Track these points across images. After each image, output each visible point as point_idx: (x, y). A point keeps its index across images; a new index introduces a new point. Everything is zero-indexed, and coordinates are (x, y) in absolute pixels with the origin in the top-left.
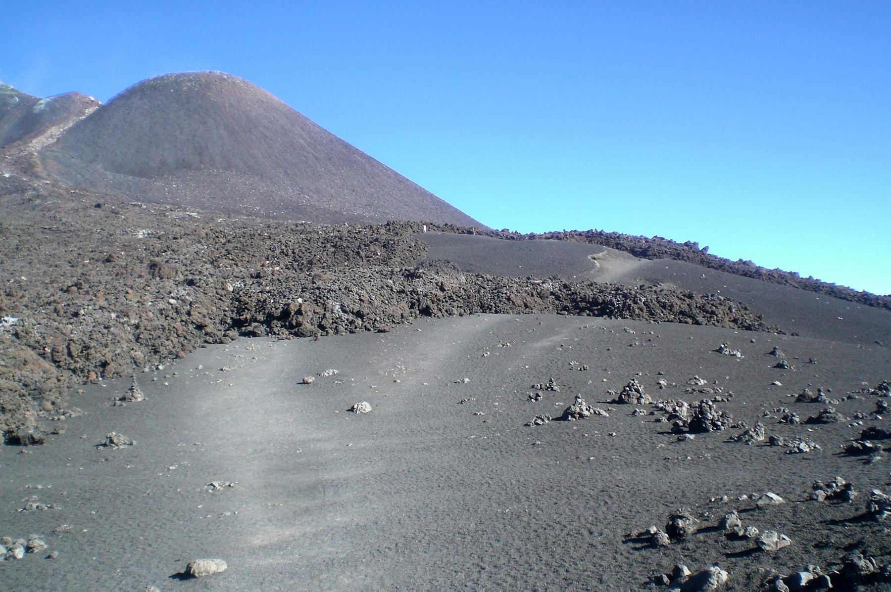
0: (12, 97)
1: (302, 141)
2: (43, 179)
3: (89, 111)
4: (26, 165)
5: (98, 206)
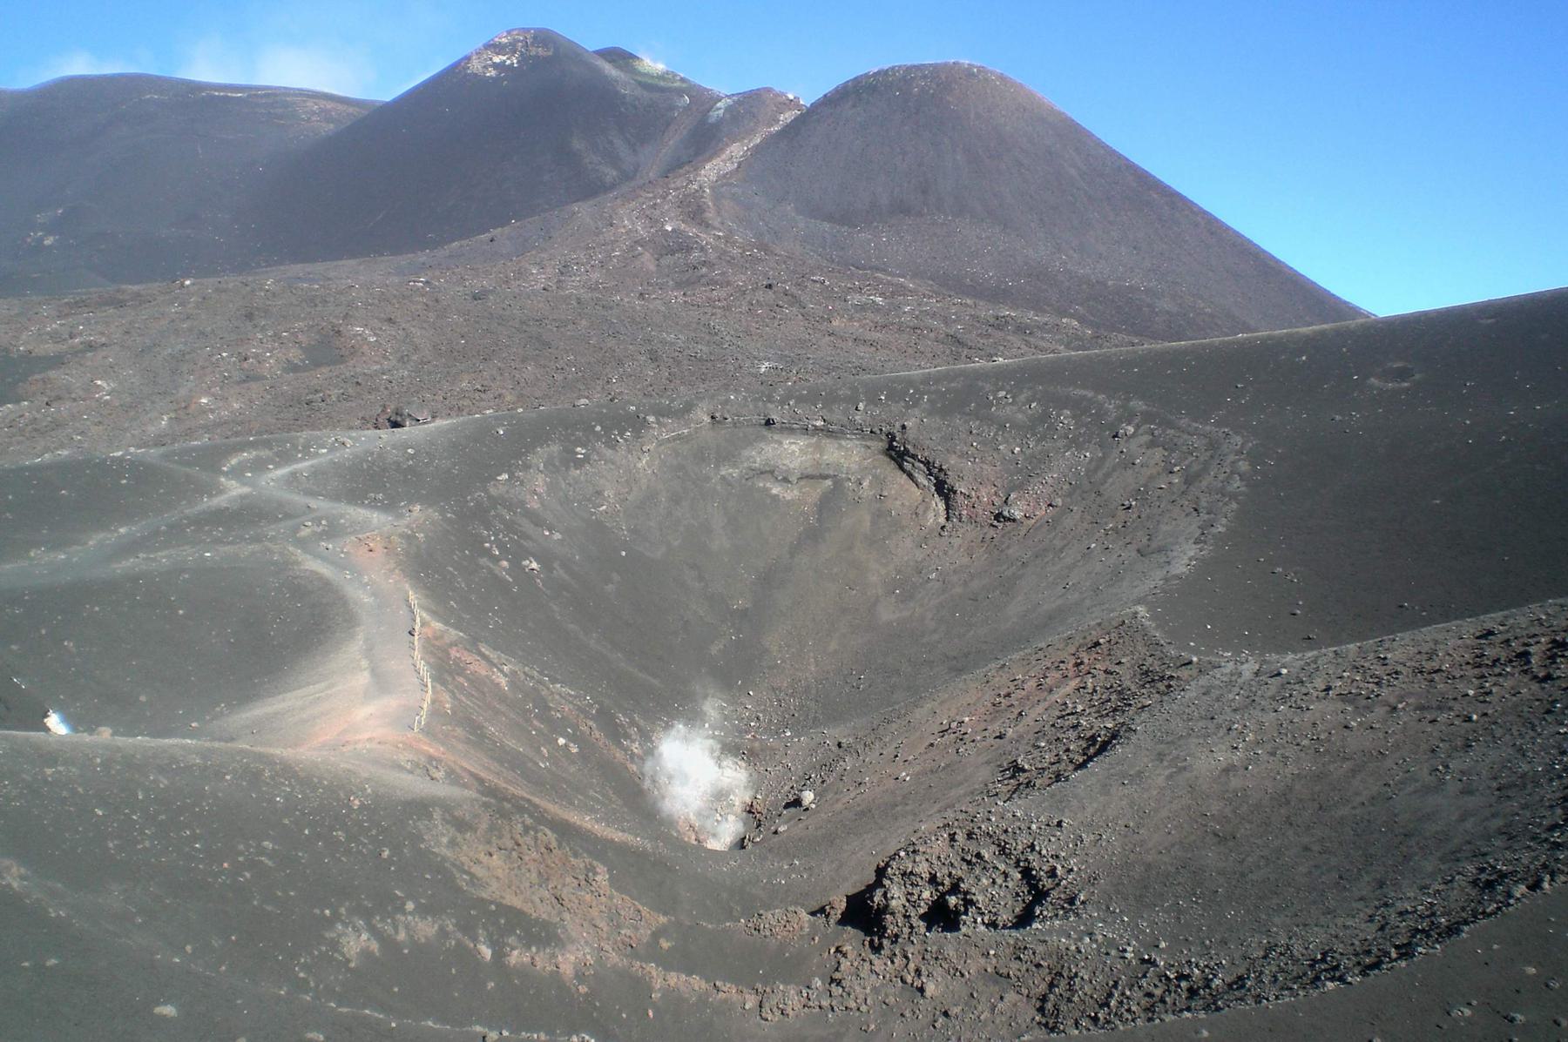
0: (680, 92)
1: (1073, 171)
3: (787, 117)
5: (770, 286)
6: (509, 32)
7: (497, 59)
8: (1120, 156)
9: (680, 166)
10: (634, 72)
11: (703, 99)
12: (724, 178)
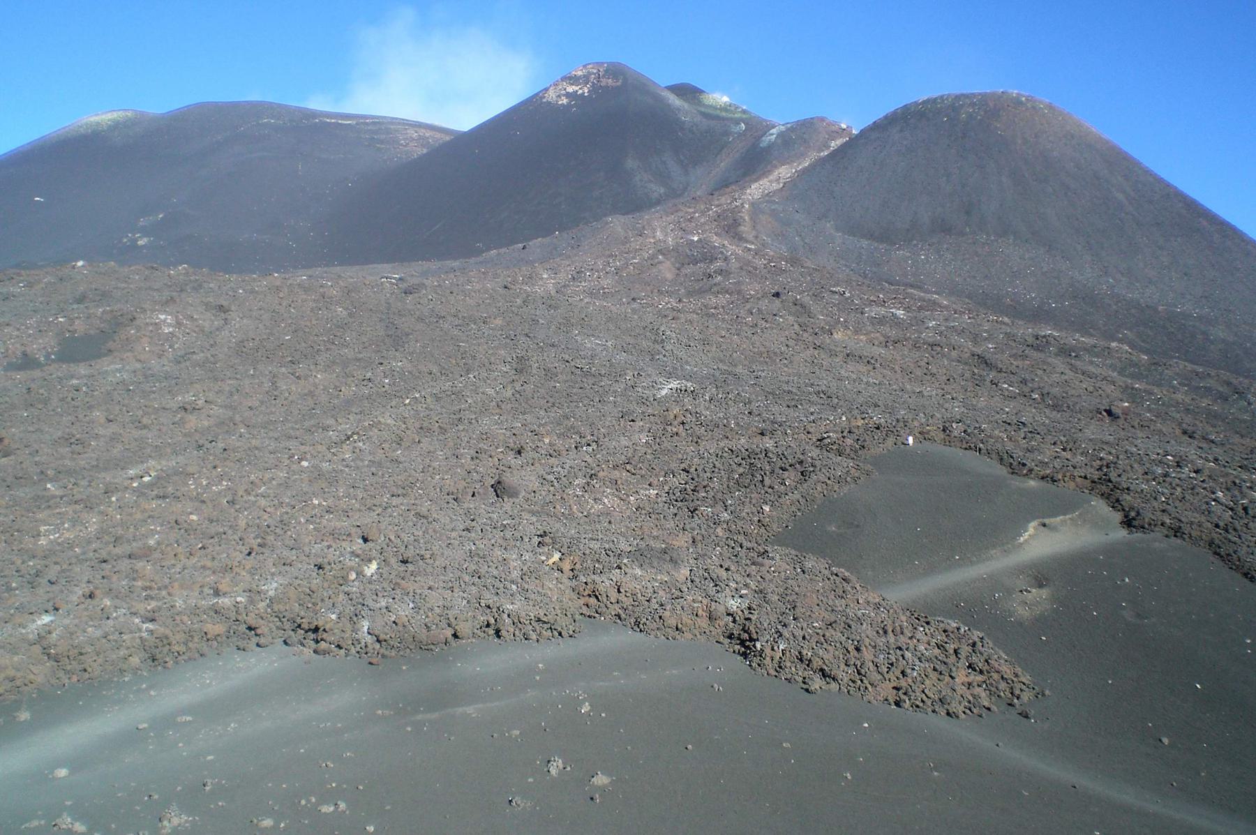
1: (1120, 196)
2: (747, 241)
3: (834, 145)
4: (731, 221)
5: (777, 295)
6: (585, 66)
7: (570, 89)
8: (1168, 185)
9: (727, 186)
10: (700, 103)
11: (757, 127)
12: (768, 197)
